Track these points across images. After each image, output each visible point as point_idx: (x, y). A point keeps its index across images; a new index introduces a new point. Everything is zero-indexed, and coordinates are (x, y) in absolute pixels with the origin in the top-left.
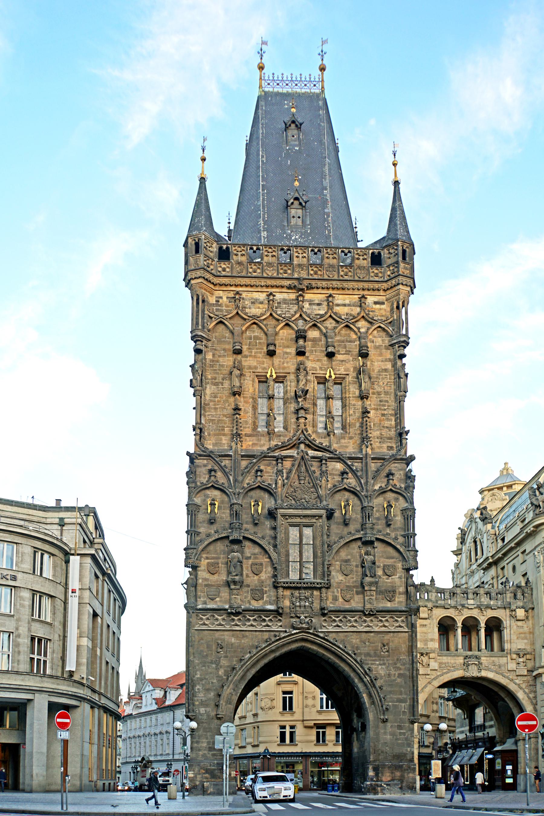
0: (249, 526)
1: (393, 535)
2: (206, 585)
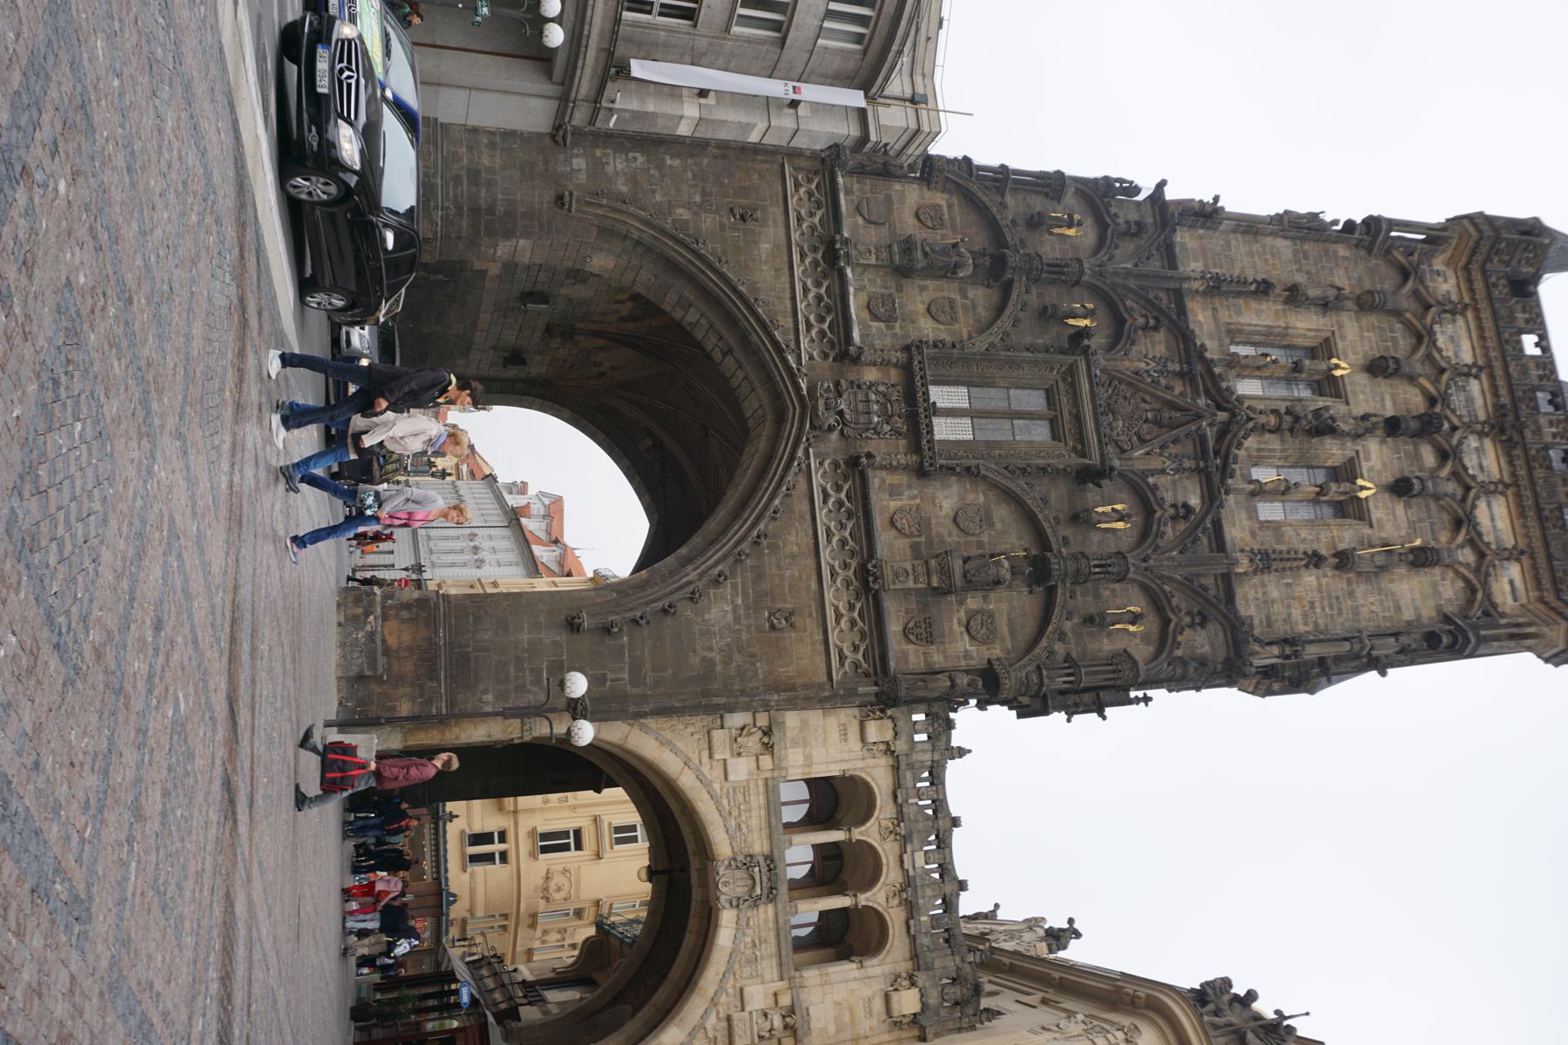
0: (1033, 299)
1: (1067, 626)
2: (888, 199)
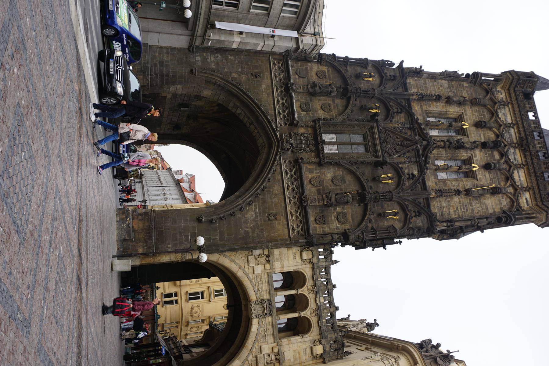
0: (358, 103)
1: (372, 217)
2: (307, 69)
